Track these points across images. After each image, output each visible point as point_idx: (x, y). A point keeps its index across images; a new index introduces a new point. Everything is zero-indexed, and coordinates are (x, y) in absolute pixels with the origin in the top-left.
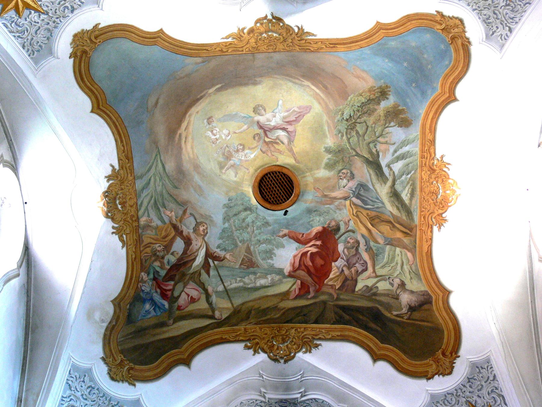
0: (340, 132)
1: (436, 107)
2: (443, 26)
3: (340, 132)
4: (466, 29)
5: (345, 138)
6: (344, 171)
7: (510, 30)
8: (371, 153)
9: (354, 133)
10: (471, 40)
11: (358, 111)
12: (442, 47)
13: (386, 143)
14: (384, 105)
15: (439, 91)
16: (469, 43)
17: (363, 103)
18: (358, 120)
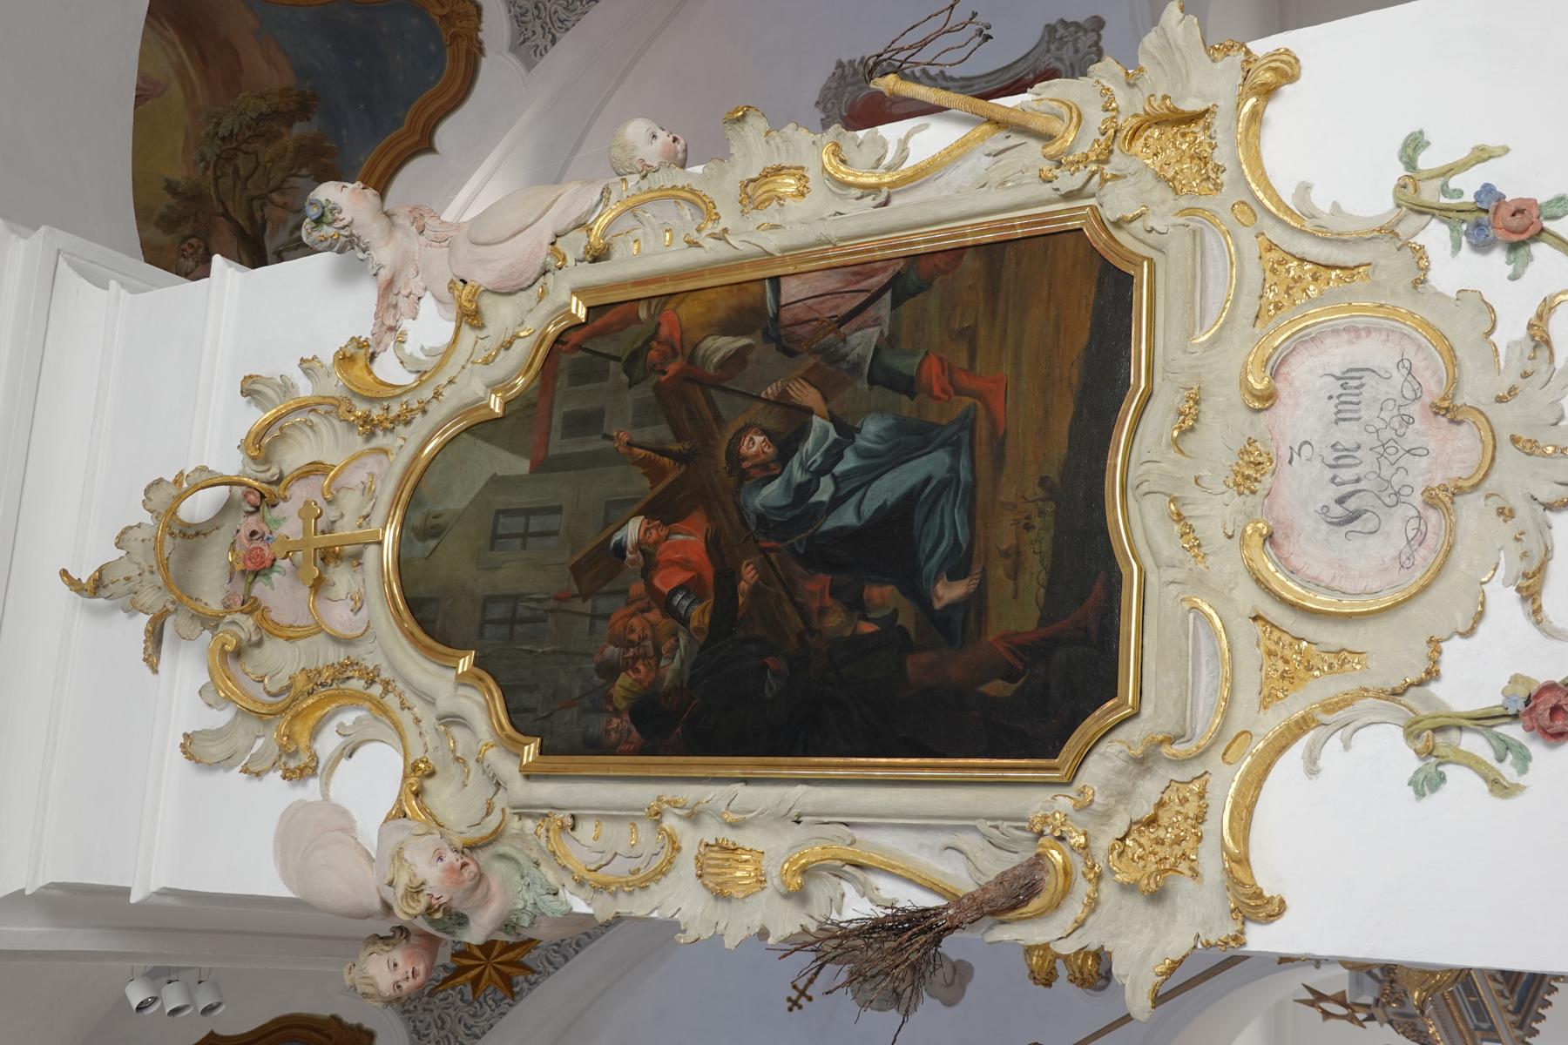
0: (203, 159)
1: (392, 155)
2: (446, 10)
3: (203, 159)
4: (483, 26)
5: (210, 173)
6: (193, 241)
7: (554, 41)
8: (251, 218)
9: (229, 170)
10: (485, 45)
11: (249, 127)
12: (433, 47)
13: (284, 206)
14: (299, 129)
15: (405, 127)
16: (481, 51)
17: (261, 114)
18: (244, 147)
